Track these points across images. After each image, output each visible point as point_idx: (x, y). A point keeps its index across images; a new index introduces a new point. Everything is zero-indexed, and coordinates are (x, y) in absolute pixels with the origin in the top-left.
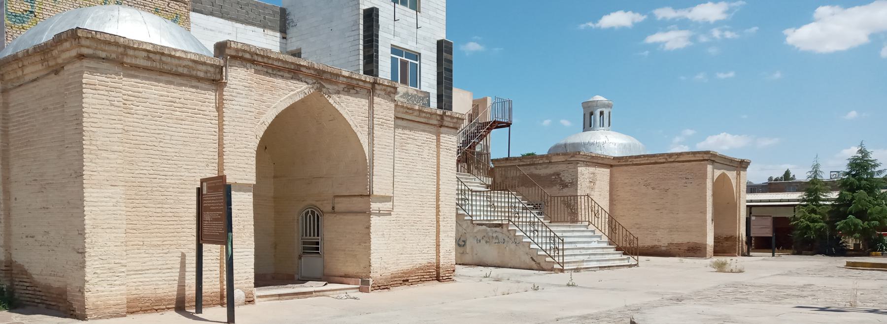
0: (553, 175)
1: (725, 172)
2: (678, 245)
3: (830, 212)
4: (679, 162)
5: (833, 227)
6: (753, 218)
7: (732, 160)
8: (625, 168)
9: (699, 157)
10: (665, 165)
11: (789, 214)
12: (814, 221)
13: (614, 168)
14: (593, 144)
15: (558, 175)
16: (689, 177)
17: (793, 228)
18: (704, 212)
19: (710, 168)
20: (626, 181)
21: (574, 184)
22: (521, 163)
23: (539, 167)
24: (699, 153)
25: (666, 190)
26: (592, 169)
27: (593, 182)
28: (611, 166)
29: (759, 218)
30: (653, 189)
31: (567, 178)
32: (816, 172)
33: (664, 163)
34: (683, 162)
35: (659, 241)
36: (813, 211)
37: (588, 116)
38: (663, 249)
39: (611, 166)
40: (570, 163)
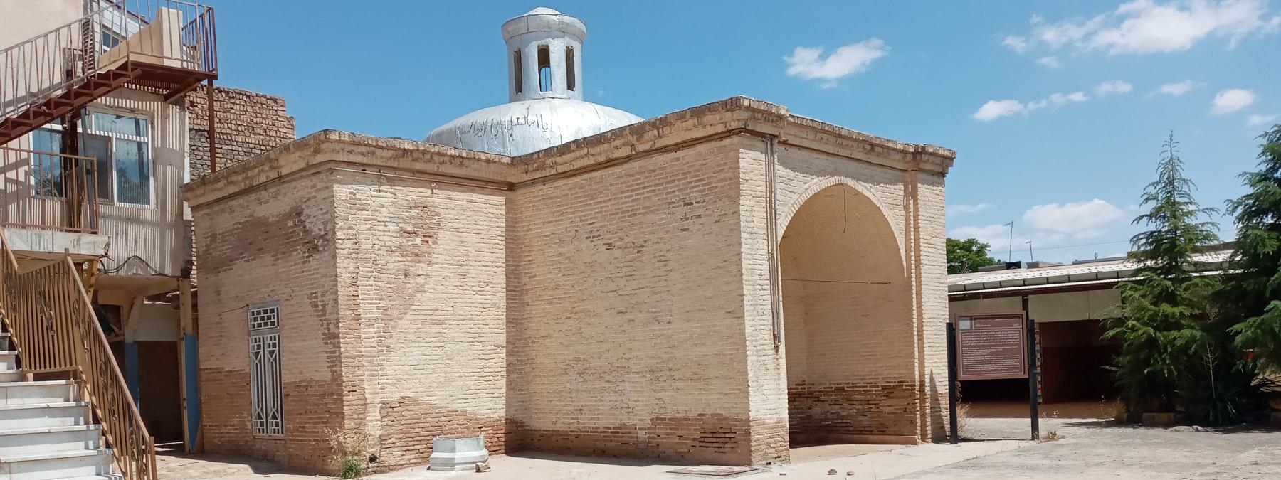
0: (288, 216)
1: (851, 182)
2: (678, 422)
3: (1217, 297)
4: (665, 150)
5: (1223, 341)
6: (964, 325)
7: (872, 146)
8: (541, 190)
9: (714, 123)
10: (634, 166)
11: (1103, 309)
12: (1168, 324)
13: (520, 194)
14: (480, 129)
17: (1116, 346)
18: (737, 313)
19: (751, 161)
20: (547, 230)
22: (232, 190)
24: (709, 108)
26: (412, 194)
27: (420, 234)
28: (511, 187)
29: (980, 324)
30: (609, 246)
32: (1171, 182)
33: (628, 159)
36: (1171, 298)
38: (642, 435)
39: (511, 187)
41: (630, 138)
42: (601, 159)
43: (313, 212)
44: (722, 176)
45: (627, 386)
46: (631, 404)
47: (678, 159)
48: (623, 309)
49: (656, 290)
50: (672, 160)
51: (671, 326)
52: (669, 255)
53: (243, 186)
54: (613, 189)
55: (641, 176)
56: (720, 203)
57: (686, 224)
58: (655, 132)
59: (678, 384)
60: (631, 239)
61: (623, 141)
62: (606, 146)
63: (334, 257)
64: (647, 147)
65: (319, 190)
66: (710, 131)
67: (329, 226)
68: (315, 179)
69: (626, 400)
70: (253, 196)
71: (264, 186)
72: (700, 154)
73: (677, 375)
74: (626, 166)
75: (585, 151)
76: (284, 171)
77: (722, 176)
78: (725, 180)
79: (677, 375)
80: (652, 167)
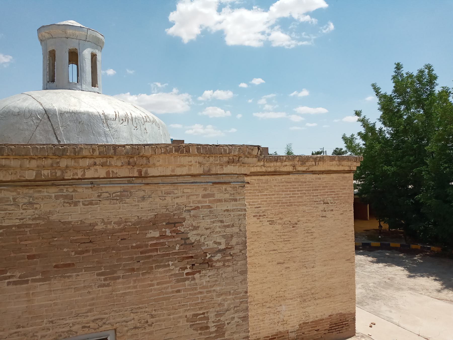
0: (154, 223)
10: (292, 177)
15: (174, 223)
16: (329, 199)
21: (233, 253)
23: (84, 191)
25: (294, 225)
30: (272, 222)
31: (206, 233)
33: (289, 173)
34: (322, 172)
35: (284, 322)
37: (63, 57)
40: (220, 181)
41: (296, 162)
42: (269, 170)
43: (206, 223)
44: (345, 191)
45: (284, 307)
46: (285, 318)
47: (320, 179)
48: (282, 261)
49: (305, 249)
50: (316, 178)
51: (315, 269)
52: (313, 230)
53: (30, 175)
54: (277, 189)
55: (296, 184)
56: (344, 205)
57: (324, 214)
58: (314, 163)
59: (318, 301)
60: (289, 219)
61: (291, 163)
62: (278, 164)
63: (244, 272)
64: (304, 169)
65: (220, 201)
66: (341, 168)
67: (234, 242)
68: (215, 190)
69: (282, 317)
70: (53, 191)
71: (93, 182)
72: (332, 178)
73: (317, 296)
74: (284, 176)
75: (262, 163)
76: (152, 172)
77: (345, 191)
78: (346, 194)
79: (317, 296)
80: (304, 180)
